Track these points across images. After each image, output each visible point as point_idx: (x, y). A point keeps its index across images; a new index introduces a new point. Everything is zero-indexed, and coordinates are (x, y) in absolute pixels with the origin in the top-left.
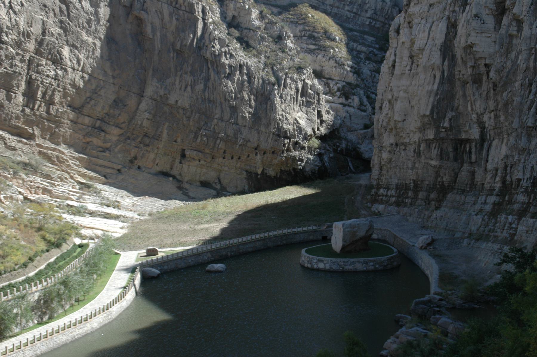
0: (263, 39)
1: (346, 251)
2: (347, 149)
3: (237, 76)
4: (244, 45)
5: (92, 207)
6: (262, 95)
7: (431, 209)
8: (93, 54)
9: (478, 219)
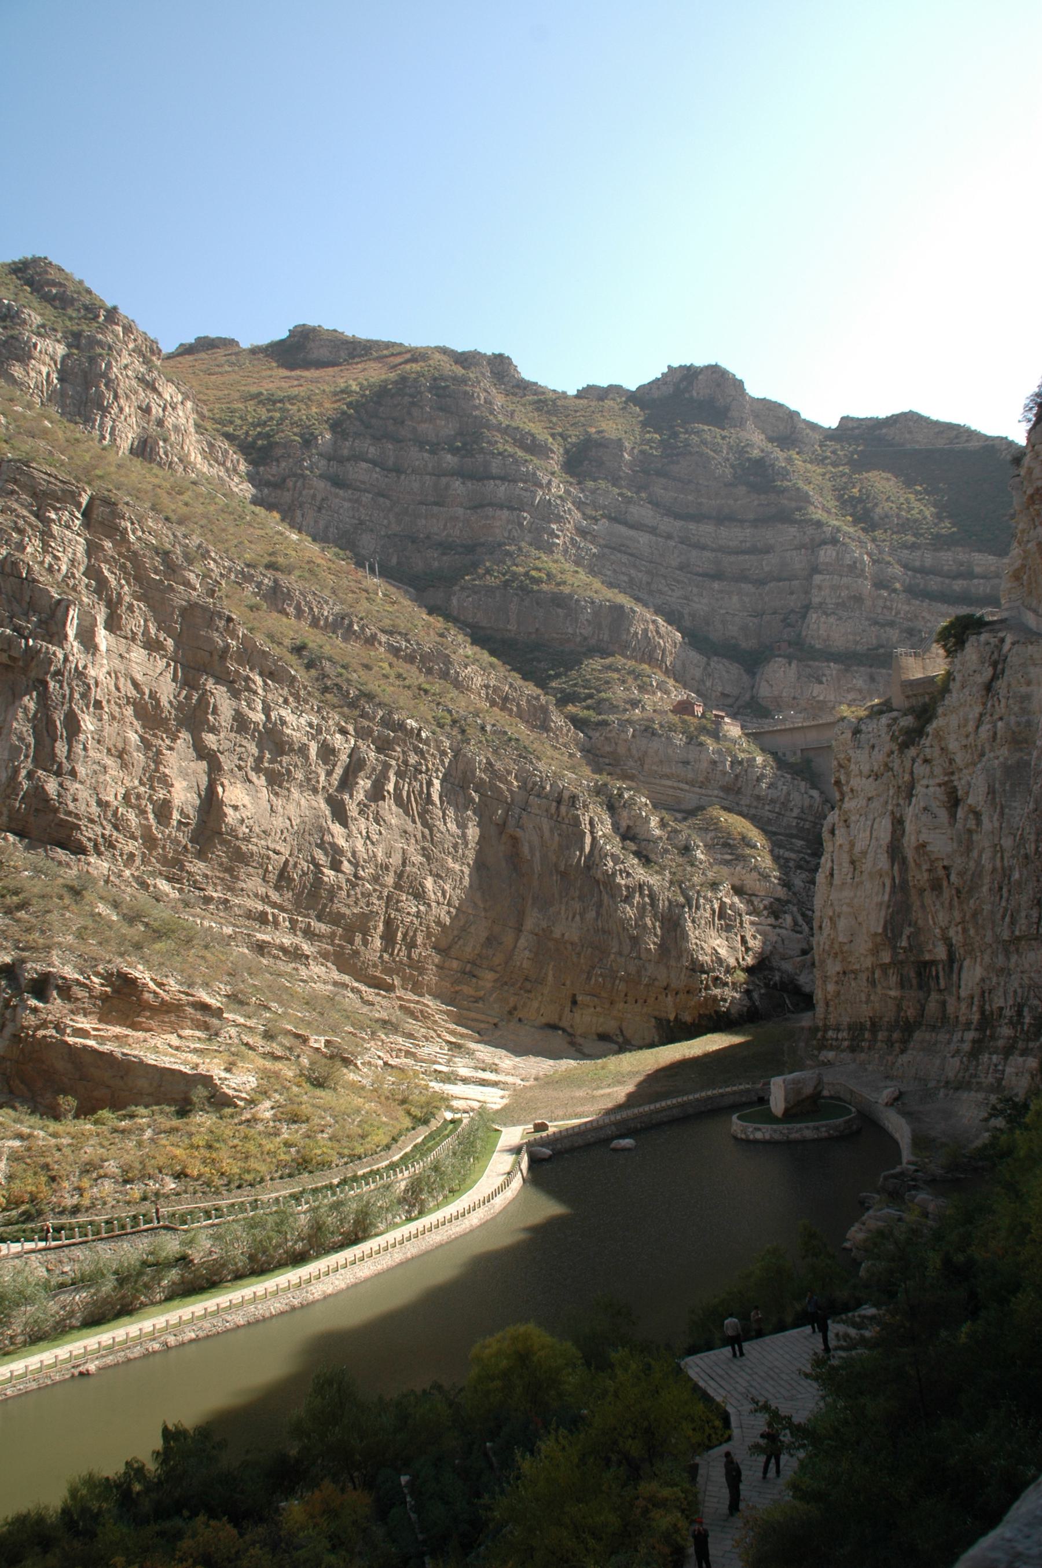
0: (666, 851)
1: (790, 1115)
2: (782, 982)
3: (637, 898)
4: (644, 860)
5: (464, 1072)
6: (669, 920)
7: (895, 1053)
8: (461, 883)
9: (956, 1061)
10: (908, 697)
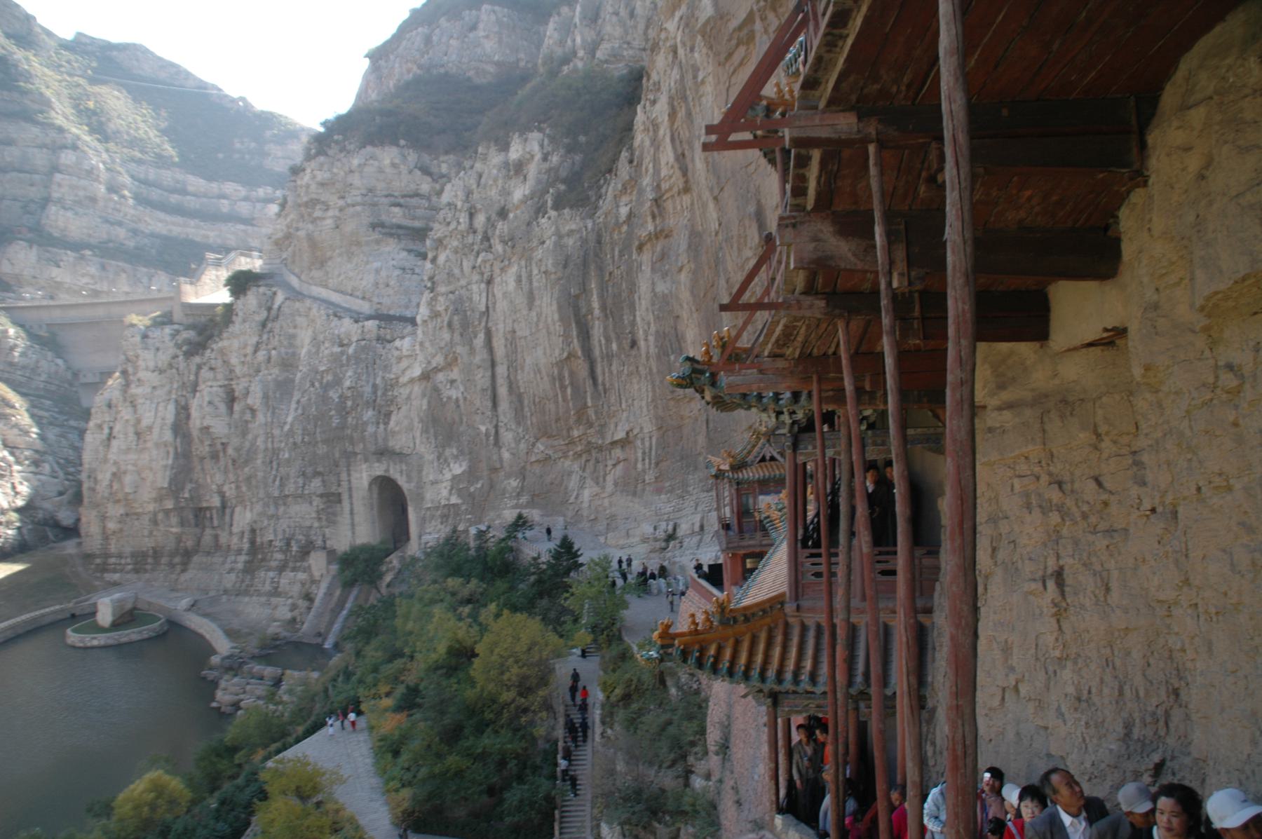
1: (116, 626)
10: (187, 315)
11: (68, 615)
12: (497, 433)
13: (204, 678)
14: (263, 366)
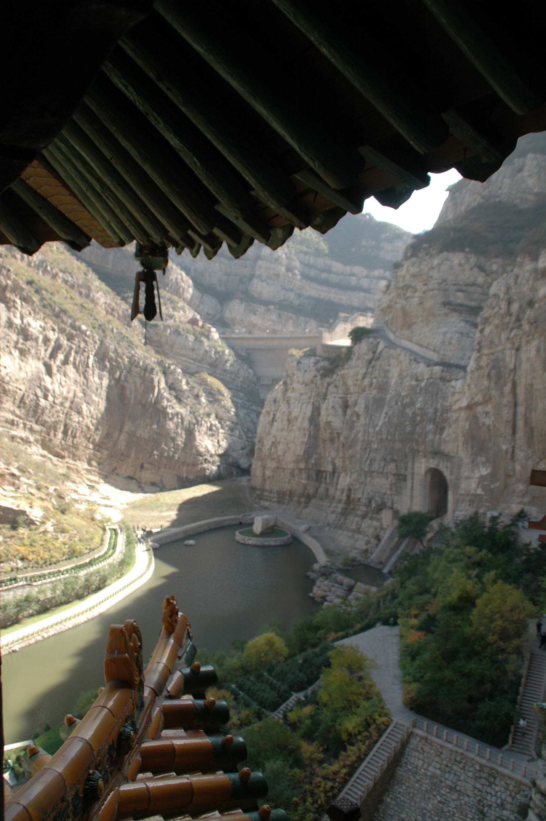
0: (189, 397)
1: (263, 534)
3: (175, 419)
9: (334, 516)
10: (324, 351)
11: (238, 522)
12: (513, 452)
13: (308, 577)
14: (367, 389)
